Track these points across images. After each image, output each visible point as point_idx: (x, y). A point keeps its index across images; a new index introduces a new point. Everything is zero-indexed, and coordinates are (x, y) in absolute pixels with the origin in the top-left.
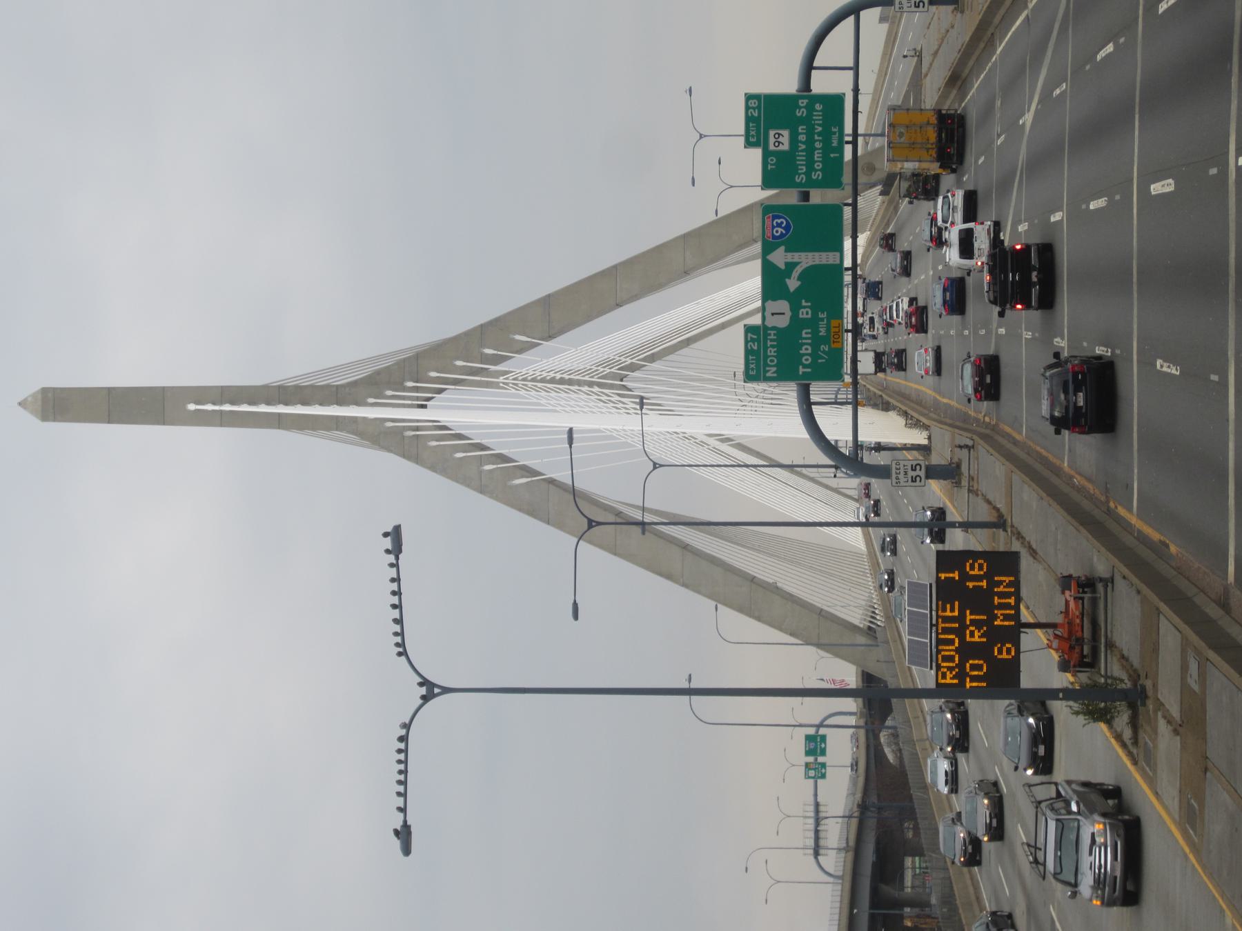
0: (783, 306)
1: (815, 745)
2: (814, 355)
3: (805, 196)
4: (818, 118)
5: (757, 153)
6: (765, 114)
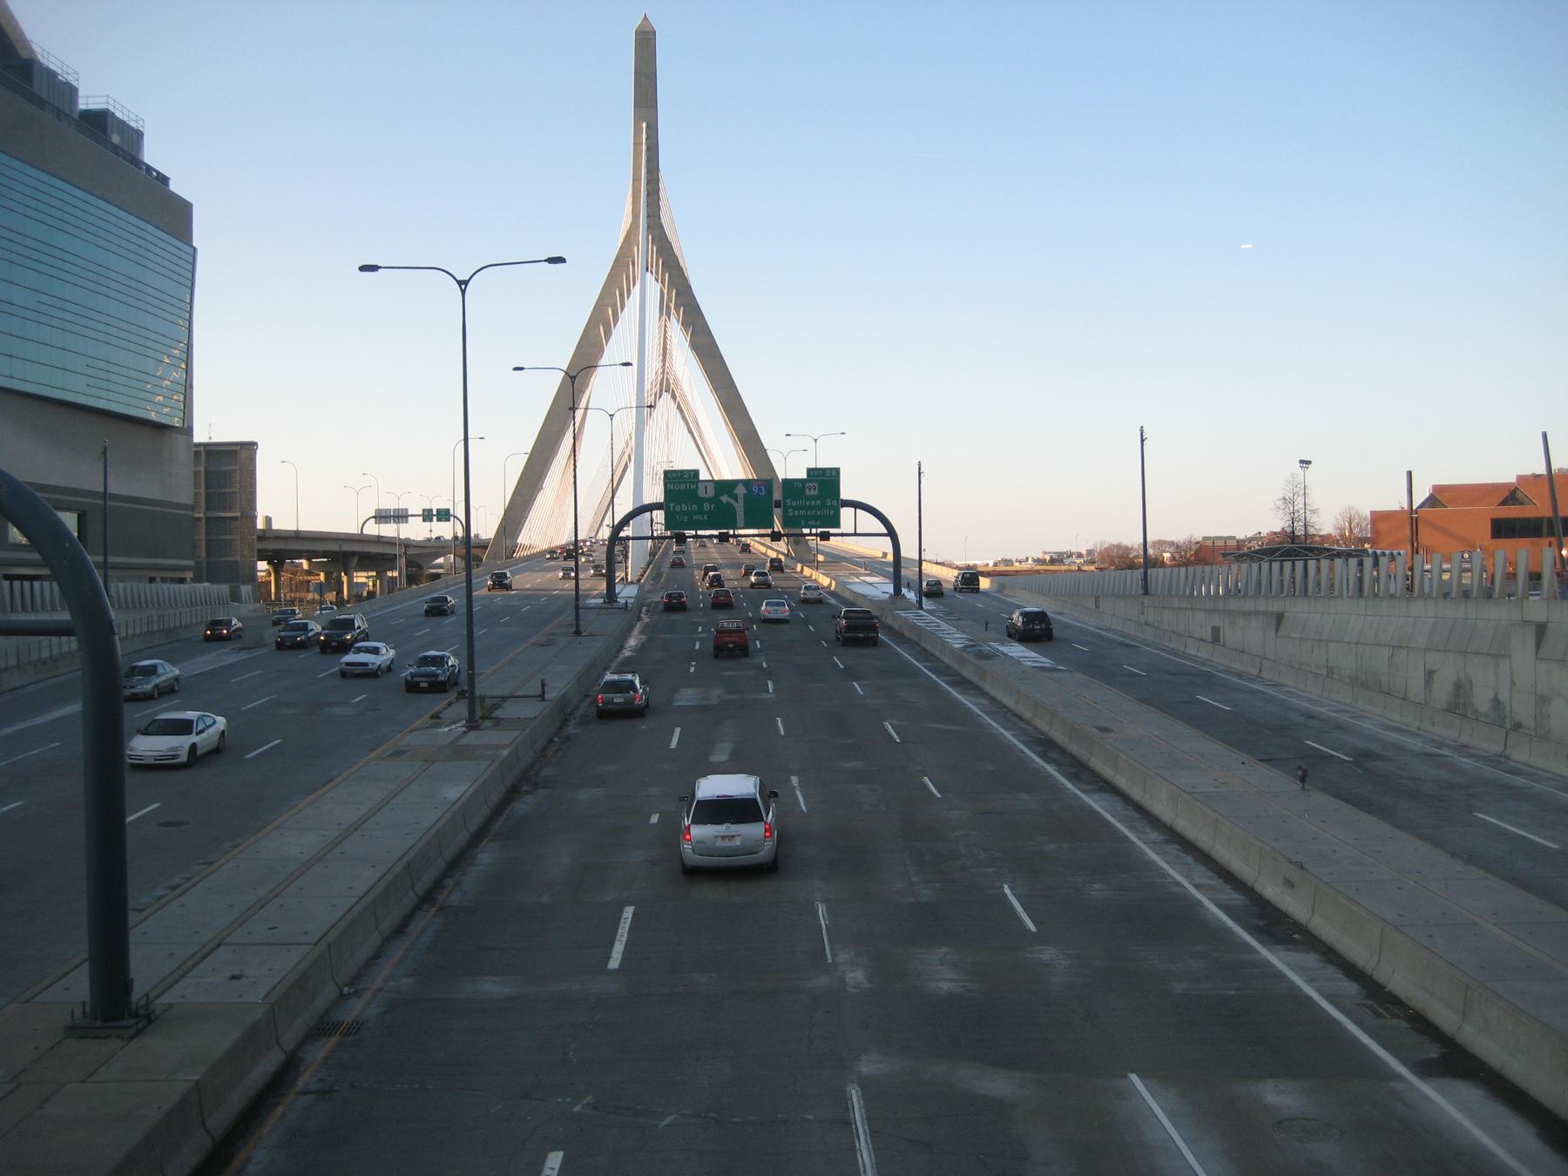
0: (711, 493)
1: (444, 515)
2: (681, 512)
3: (778, 505)
4: (826, 512)
5: (804, 476)
6: (825, 482)
